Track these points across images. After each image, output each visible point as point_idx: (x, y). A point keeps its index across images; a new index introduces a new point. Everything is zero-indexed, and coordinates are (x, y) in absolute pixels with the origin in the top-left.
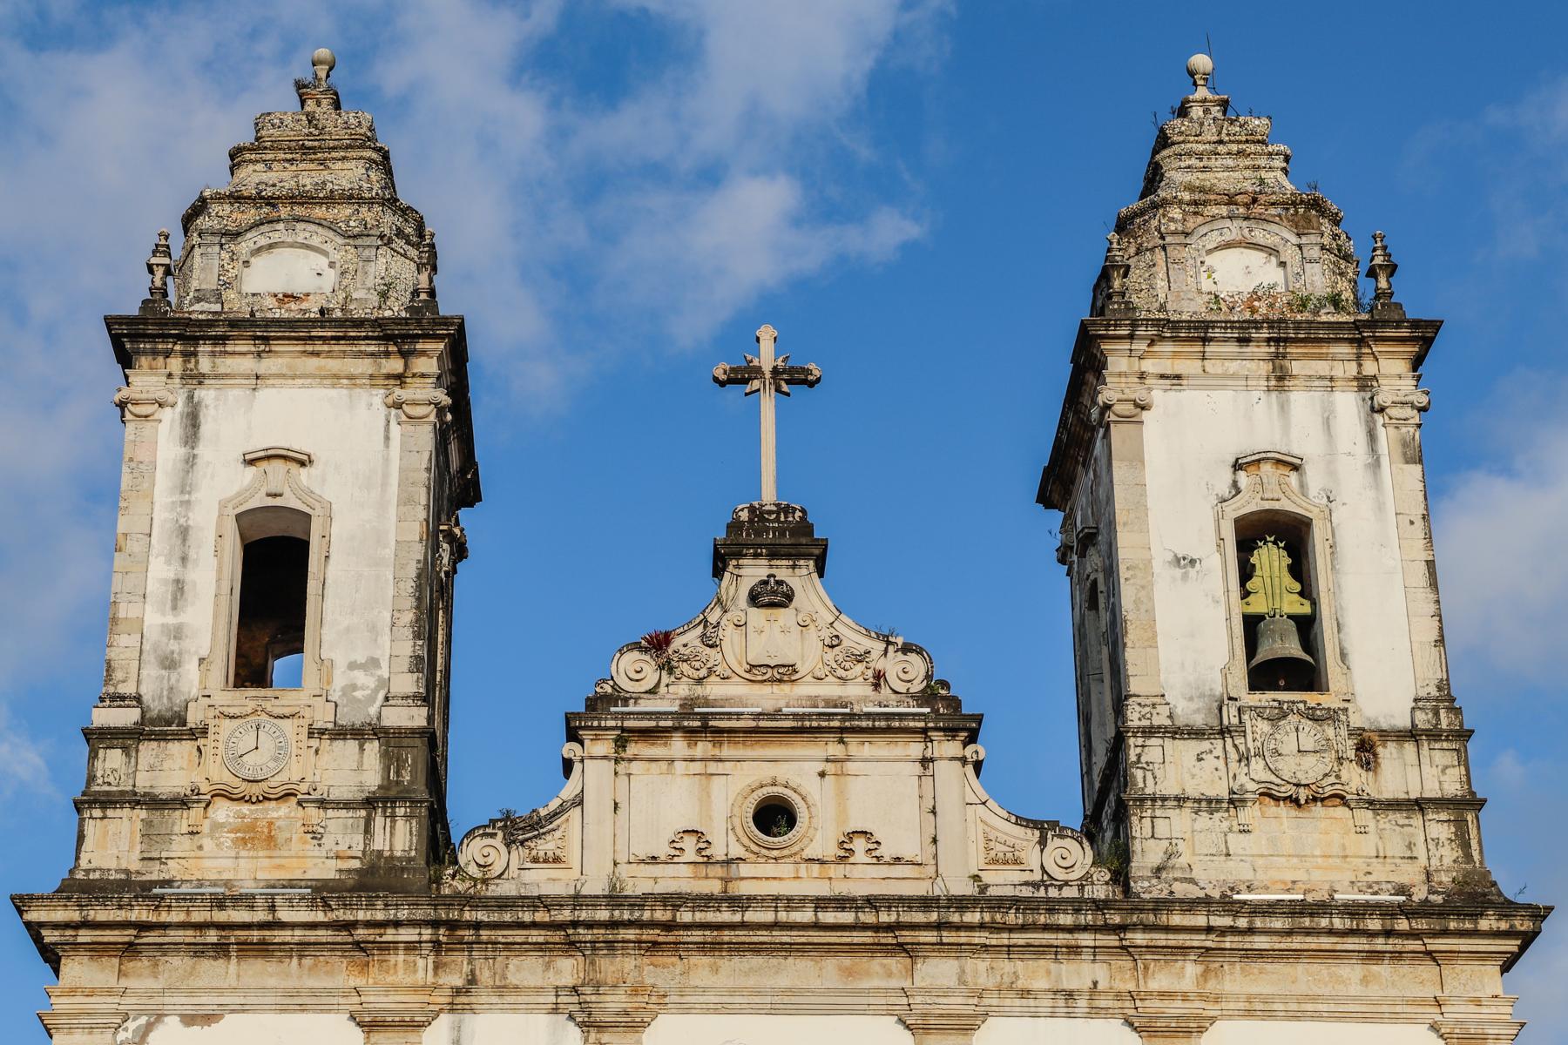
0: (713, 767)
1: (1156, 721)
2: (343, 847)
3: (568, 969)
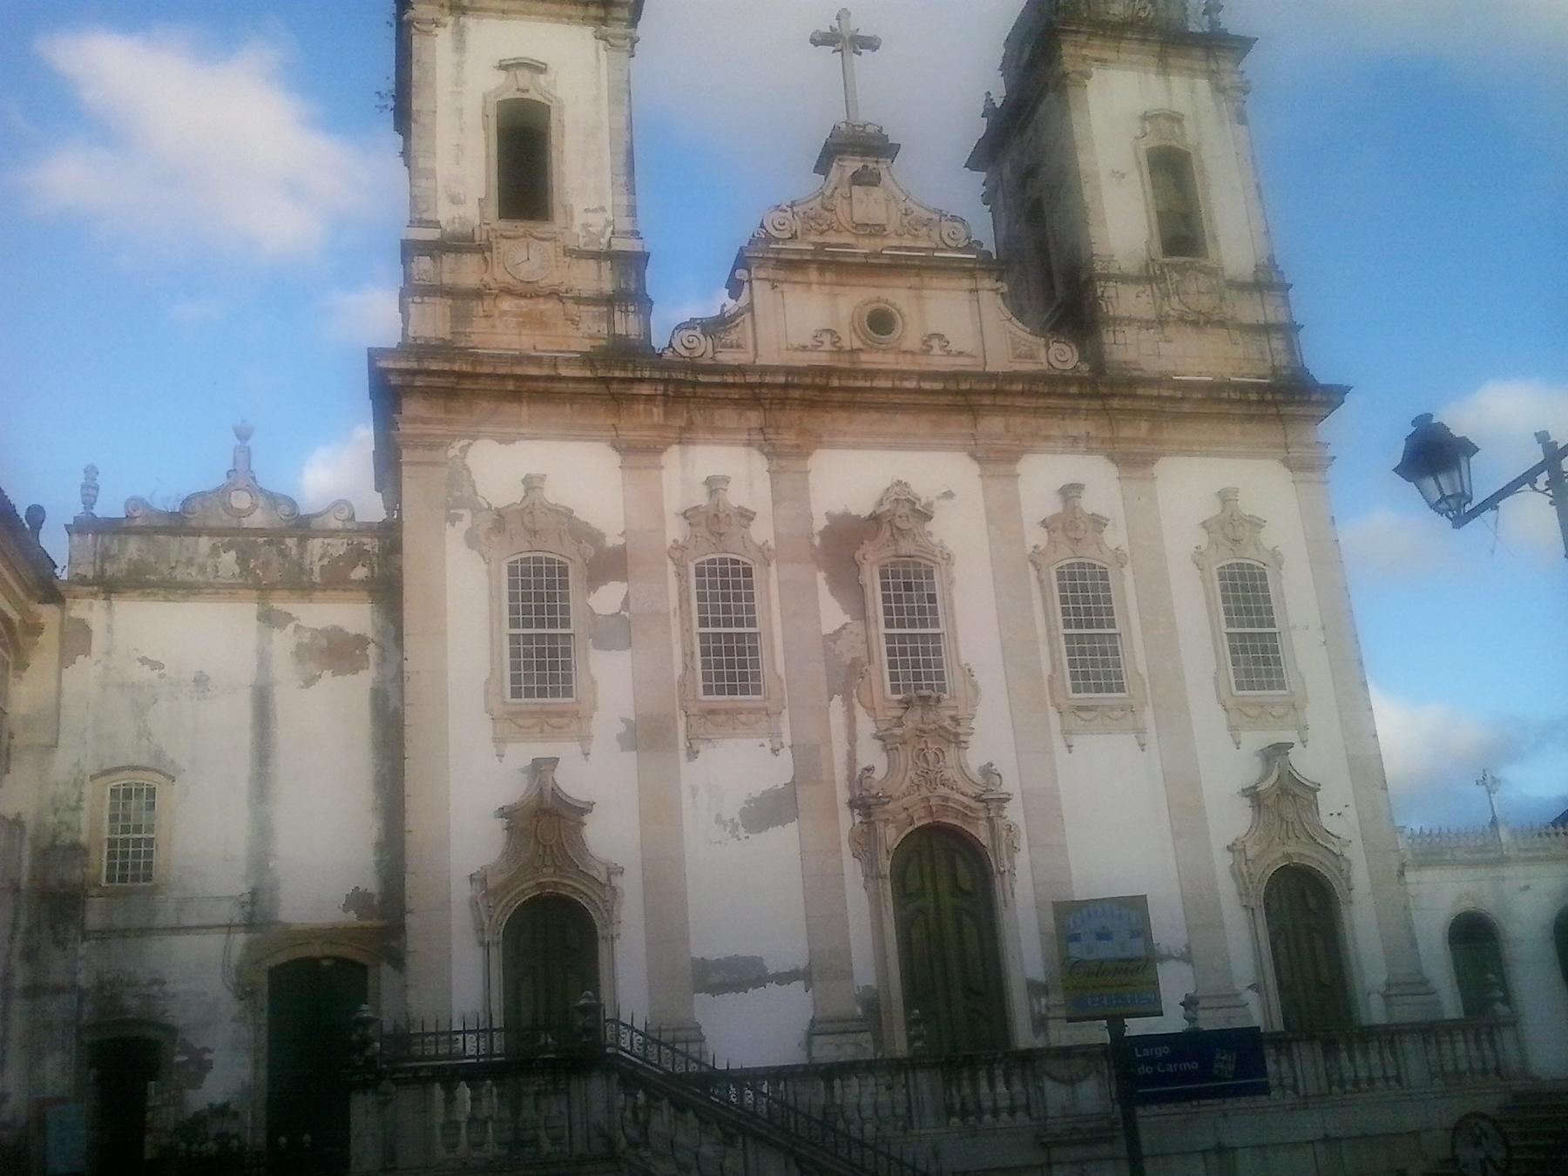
0: (838, 289)
3: (754, 417)
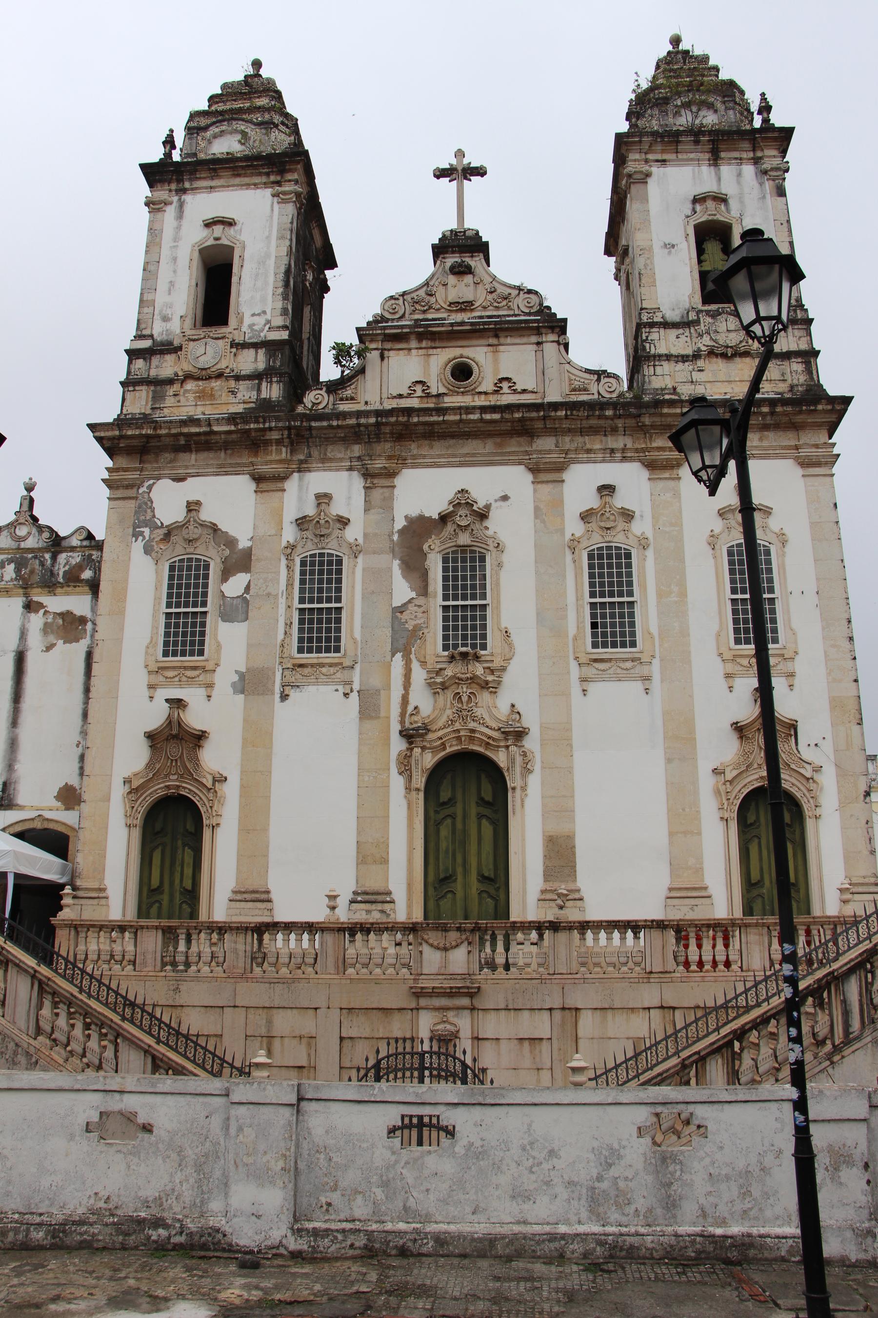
0: (431, 351)
1: (655, 320)
2: (247, 397)
3: (357, 450)
